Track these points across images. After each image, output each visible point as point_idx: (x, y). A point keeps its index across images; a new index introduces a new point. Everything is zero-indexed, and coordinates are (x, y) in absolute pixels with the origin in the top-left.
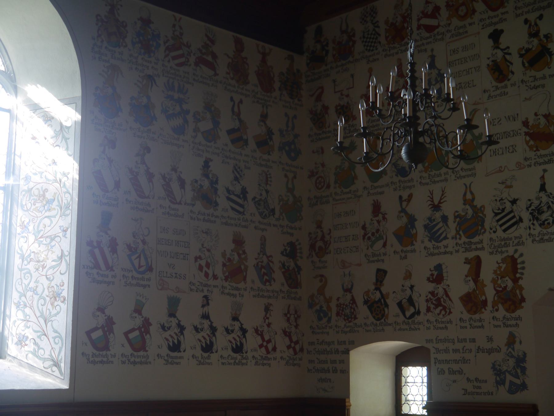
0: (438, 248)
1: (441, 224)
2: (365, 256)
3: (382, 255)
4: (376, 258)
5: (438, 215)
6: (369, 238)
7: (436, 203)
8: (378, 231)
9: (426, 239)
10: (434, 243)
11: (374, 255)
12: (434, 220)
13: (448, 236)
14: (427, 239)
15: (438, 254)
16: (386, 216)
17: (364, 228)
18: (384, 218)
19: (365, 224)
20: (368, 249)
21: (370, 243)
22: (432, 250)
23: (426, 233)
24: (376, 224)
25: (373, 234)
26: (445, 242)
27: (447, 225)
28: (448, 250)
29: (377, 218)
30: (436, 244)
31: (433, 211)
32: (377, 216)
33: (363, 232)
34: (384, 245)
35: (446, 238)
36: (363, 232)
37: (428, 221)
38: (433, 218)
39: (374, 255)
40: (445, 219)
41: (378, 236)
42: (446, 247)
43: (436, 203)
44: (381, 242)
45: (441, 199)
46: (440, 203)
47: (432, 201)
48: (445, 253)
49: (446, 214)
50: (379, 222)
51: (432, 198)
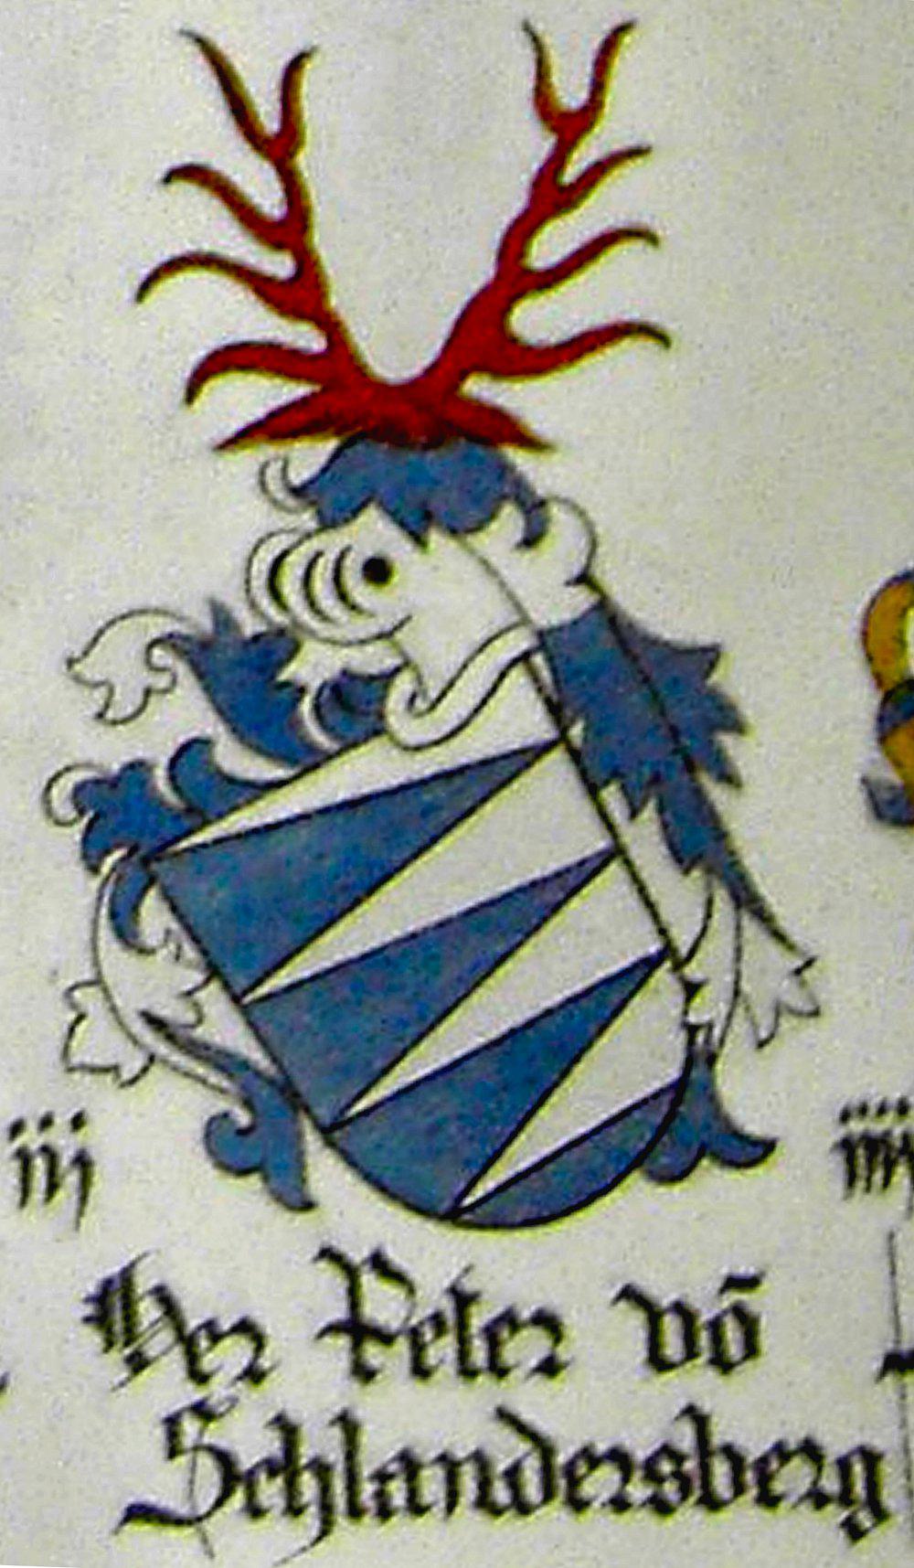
0: (473, 1336)
1: (542, 821)
5: (454, 617)
7: (397, 336)
9: (155, 1130)
10: (351, 1209)
12: (354, 706)
13: (745, 1091)
14: (180, 1106)
15: (495, 1492)
22: (310, 1381)
23: (161, 976)
26: (664, 1231)
27: (701, 844)
28: (747, 1412)
30: (435, 1255)
31: (328, 501)
35: (683, 1131)
37: (186, 713)
38: (312, 667)
40: (640, 712)
42: (710, 1332)
43: (397, 336)
45: (515, 277)
46: (482, 336)
47: (301, 294)
48: (690, 1474)
49: (662, 612)
51: (289, 231)
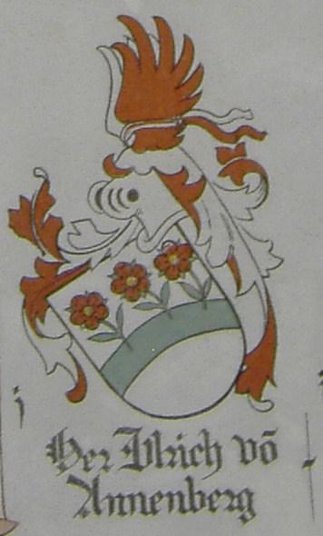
2: (55, 450)
3: (231, 453)
4: (170, 479)
6: (89, 311)
8: (177, 259)
11: (142, 451)
16: (253, 149)
17: (34, 218)
18: (236, 165)
19: (45, 198)
20: (77, 394)
21: (101, 352)
24: (158, 204)
25: (129, 280)
29: (169, 160)
32: (171, 139)
33: (24, 256)
34: (255, 374)
36: (24, 256)
39: (142, 451)
41: (178, 296)
44: (222, 354)
50: (184, 190)
